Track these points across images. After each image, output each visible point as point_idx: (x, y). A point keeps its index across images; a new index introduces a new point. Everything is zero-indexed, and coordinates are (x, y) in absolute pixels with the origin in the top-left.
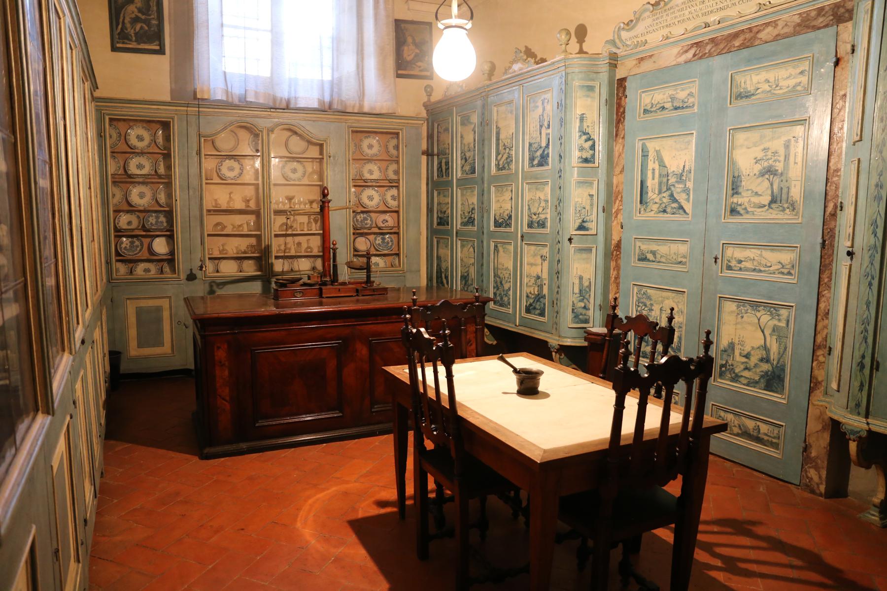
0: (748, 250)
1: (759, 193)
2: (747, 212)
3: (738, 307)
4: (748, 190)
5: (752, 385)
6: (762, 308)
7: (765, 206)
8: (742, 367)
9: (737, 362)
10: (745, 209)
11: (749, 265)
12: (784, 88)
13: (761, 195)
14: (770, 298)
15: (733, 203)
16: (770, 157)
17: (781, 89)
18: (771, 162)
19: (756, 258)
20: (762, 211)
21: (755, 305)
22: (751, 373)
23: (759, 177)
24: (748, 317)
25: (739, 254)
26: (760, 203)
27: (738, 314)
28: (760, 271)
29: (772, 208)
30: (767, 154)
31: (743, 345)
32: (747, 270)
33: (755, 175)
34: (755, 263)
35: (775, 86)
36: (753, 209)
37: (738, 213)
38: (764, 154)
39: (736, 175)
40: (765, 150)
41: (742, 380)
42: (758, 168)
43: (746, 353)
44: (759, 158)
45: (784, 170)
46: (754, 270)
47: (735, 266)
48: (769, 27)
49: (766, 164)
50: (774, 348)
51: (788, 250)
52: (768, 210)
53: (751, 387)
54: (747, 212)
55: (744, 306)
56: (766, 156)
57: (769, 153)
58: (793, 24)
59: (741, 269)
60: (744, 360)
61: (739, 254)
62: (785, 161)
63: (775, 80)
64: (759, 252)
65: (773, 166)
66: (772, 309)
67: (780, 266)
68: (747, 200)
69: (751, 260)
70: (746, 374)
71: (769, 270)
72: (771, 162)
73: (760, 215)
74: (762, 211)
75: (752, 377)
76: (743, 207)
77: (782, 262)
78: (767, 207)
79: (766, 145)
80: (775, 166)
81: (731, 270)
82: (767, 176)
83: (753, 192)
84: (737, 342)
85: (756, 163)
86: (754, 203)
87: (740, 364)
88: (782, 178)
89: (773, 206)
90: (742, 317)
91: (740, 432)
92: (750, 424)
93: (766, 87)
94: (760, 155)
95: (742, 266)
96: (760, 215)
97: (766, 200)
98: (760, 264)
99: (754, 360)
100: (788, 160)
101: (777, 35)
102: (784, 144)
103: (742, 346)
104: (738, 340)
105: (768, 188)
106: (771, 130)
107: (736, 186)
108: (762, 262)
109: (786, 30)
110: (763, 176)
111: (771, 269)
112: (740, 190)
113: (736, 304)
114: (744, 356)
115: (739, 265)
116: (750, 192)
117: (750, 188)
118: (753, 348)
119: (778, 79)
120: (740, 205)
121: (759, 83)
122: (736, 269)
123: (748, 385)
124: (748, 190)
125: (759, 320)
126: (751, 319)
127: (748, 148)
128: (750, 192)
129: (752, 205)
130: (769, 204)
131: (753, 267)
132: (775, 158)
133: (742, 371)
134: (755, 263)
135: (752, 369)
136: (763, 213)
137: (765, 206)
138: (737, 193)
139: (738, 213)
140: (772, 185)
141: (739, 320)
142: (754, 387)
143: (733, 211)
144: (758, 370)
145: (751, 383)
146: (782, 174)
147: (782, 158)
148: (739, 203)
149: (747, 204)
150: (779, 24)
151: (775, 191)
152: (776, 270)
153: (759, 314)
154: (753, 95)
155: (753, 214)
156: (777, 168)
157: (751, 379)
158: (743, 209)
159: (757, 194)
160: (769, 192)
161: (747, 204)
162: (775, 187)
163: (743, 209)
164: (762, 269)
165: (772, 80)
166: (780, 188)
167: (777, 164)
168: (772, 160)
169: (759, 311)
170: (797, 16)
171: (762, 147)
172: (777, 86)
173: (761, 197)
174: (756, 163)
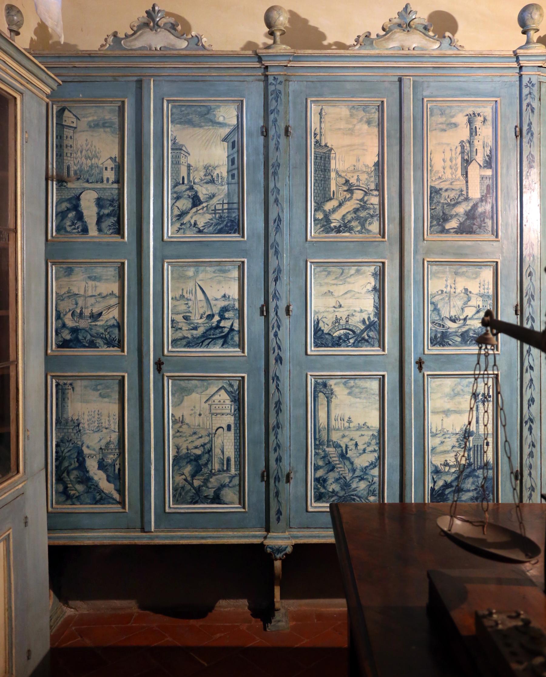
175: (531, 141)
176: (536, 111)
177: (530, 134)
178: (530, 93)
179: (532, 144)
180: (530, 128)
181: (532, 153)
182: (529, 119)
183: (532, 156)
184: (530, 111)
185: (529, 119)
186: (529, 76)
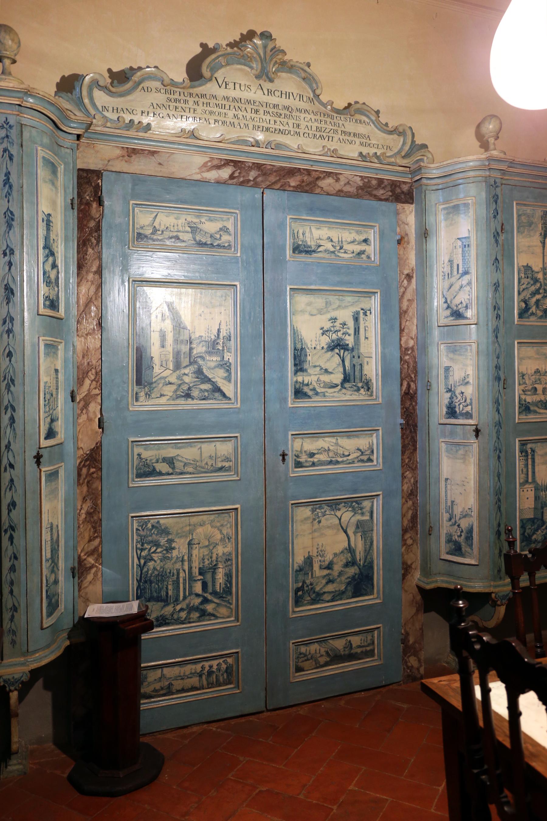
0: (321, 439)
1: (330, 370)
2: (317, 394)
3: (313, 511)
4: (315, 366)
5: (338, 597)
6: (343, 504)
7: (337, 386)
8: (324, 581)
9: (318, 578)
10: (314, 389)
11: (323, 457)
12: (349, 252)
13: (331, 373)
14: (355, 491)
15: (296, 382)
16: (338, 328)
17: (345, 252)
18: (340, 334)
19: (331, 448)
20: (335, 392)
21: (334, 505)
22: (335, 585)
23: (328, 351)
24: (327, 520)
25: (310, 445)
26: (331, 382)
27: (314, 519)
28: (337, 462)
29: (345, 388)
30: (335, 324)
31: (323, 555)
32: (322, 463)
33: (323, 348)
34: (331, 454)
35: (338, 248)
36: (323, 390)
37: (306, 395)
38: (332, 325)
39: (299, 346)
40: (334, 320)
41: (327, 597)
42: (325, 341)
43: (327, 563)
44: (325, 329)
45: (355, 344)
46: (331, 462)
47: (306, 461)
48: (330, 178)
49: (334, 337)
50: (359, 545)
51: (366, 434)
52: (341, 390)
53: (337, 600)
54: (317, 394)
55: (320, 508)
56: (333, 327)
57: (337, 324)
58: (356, 185)
59: (314, 464)
60: (326, 572)
61: (310, 445)
62: (355, 334)
63: (339, 241)
64: (334, 440)
65: (342, 339)
66: (354, 504)
67: (359, 453)
68: (314, 378)
69: (325, 450)
70: (330, 588)
71: (347, 460)
72: (340, 334)
73: (333, 397)
74: (335, 392)
75: (337, 589)
76: (311, 387)
77: (361, 448)
78: (339, 387)
79: (333, 314)
80: (346, 340)
81: (302, 467)
82: (337, 351)
83: (322, 369)
84: (315, 554)
85: (323, 334)
86: (324, 382)
87: (321, 579)
88: (354, 353)
89: (347, 385)
90: (319, 522)
91: (328, 659)
92: (339, 644)
93: (329, 246)
94: (327, 325)
95: (316, 460)
96: (333, 397)
97: (338, 378)
98: (336, 454)
99: (337, 568)
100: (359, 334)
101: (341, 191)
102: (353, 316)
103: (322, 556)
104: (316, 551)
105: (339, 365)
106: (337, 297)
107: (300, 361)
108: (339, 452)
109: (347, 189)
110: (332, 350)
111: (349, 458)
112: (306, 366)
113: (310, 508)
114: (324, 569)
115: (312, 460)
116: (318, 369)
117: (317, 364)
118: (335, 555)
119: (342, 241)
120: (307, 385)
121: (320, 239)
122: (308, 465)
123: (332, 600)
124: (315, 366)
125: (340, 520)
126: (331, 521)
127: (312, 315)
128: (318, 369)
129: (322, 385)
130: (342, 384)
131: (329, 459)
132: (344, 330)
133: (324, 586)
134: (331, 454)
135: (336, 579)
136: (335, 394)
137: (337, 386)
138: (302, 370)
139: (306, 395)
140: (343, 361)
141: (316, 526)
142: (341, 599)
143: (299, 393)
144: (343, 578)
145: (337, 596)
146: (353, 350)
147: (352, 331)
148: (306, 382)
149: (315, 384)
150: (341, 179)
151: (347, 368)
152: (355, 458)
153: (339, 514)
154: (314, 251)
155: (324, 396)
156: (347, 342)
157: (336, 591)
158: (311, 390)
159: (326, 371)
160: (341, 369)
161: (315, 384)
162: (347, 363)
163: (311, 390)
164: (340, 459)
165: (335, 239)
166: (352, 365)
167: (347, 337)
168: (342, 332)
169: (339, 510)
170: (359, 179)
171: (329, 316)
172: (341, 248)
173: (332, 375)
174: (323, 334)
175: (9, 194)
176: (15, 159)
177: (7, 186)
178: (7, 136)
179: (11, 198)
180: (9, 179)
181: (11, 209)
182: (7, 168)
183: (12, 213)
184: (8, 158)
185: (7, 168)
186: (5, 116)
